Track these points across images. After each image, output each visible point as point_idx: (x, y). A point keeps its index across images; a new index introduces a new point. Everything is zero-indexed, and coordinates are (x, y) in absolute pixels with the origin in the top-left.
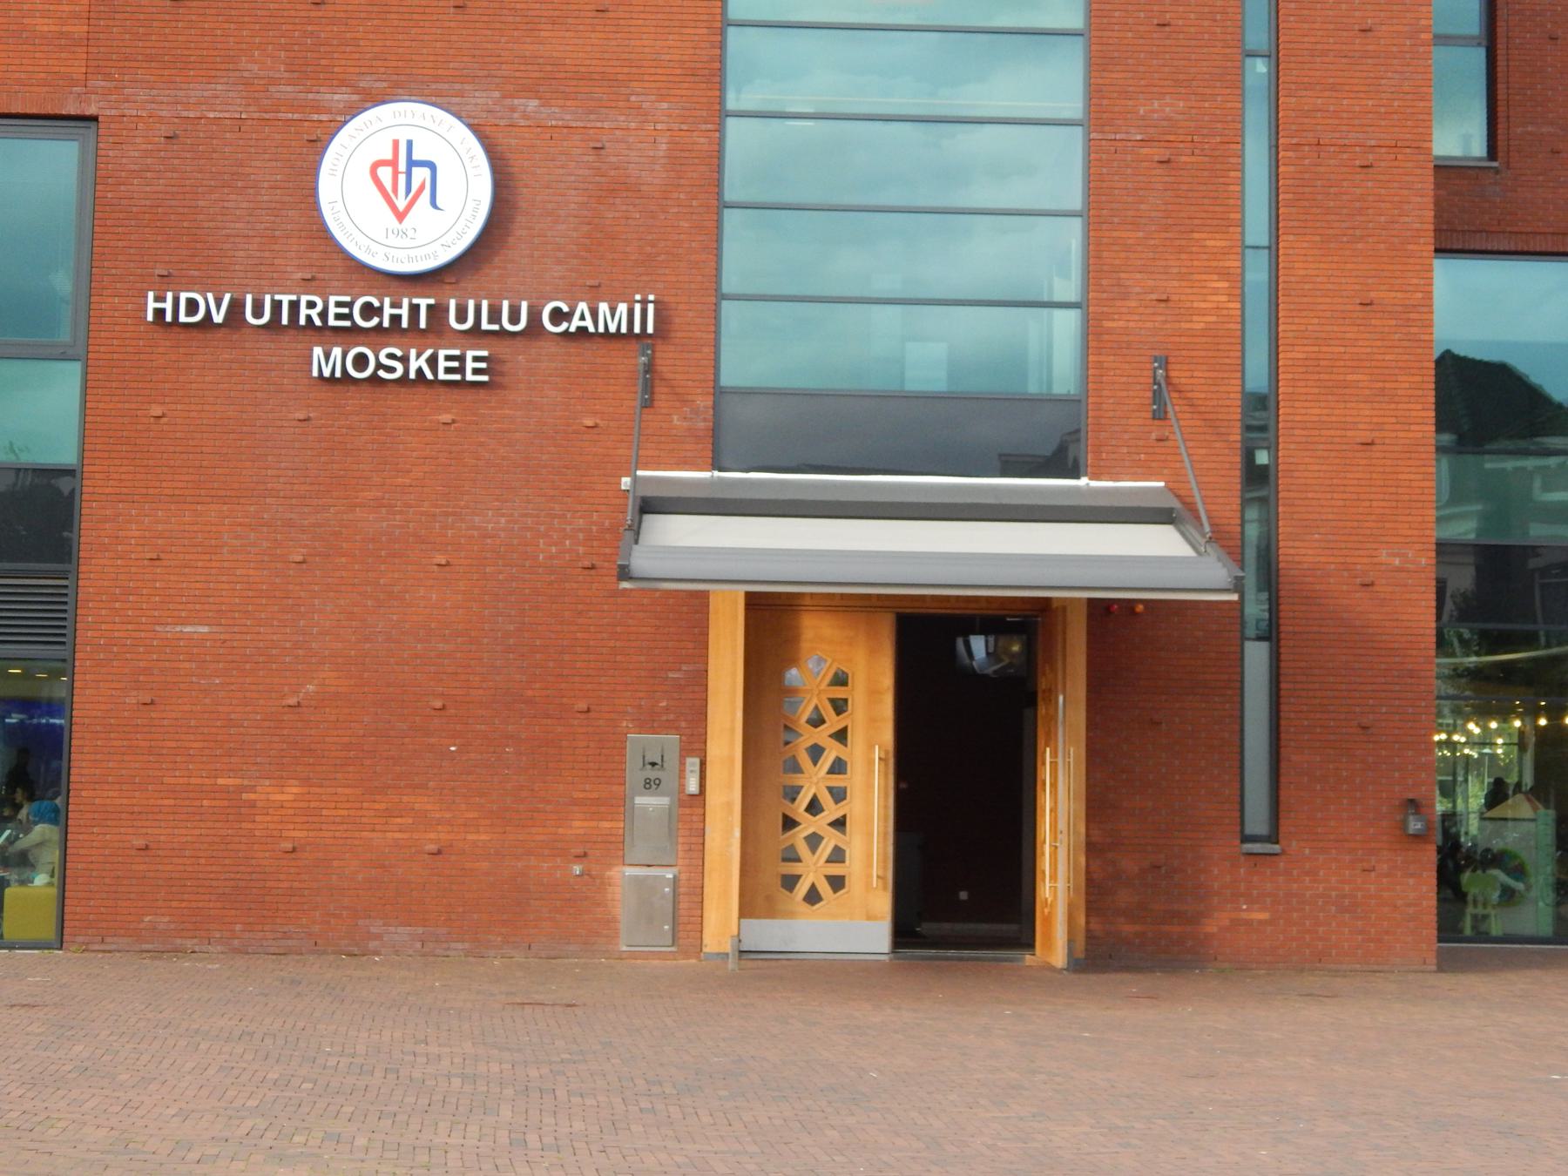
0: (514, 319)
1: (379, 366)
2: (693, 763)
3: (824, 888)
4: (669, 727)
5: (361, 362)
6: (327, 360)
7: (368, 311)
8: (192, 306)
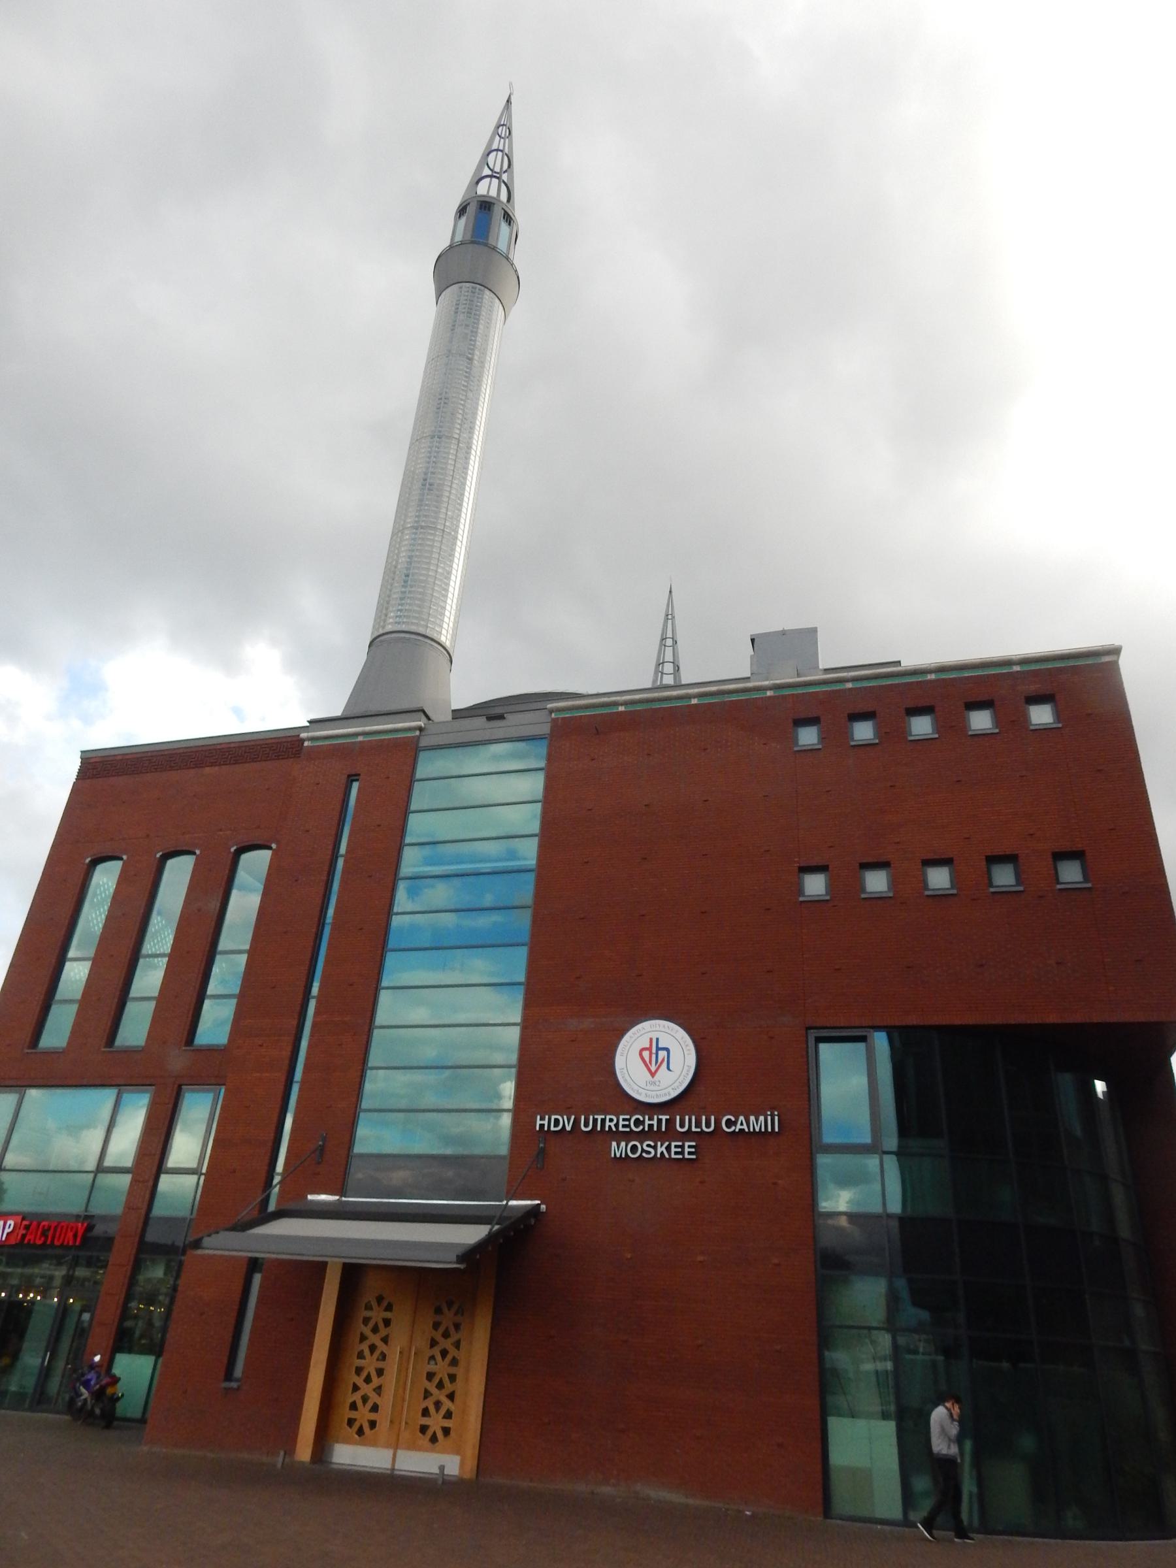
1: (643, 1150)
6: (618, 1149)
7: (638, 1123)
8: (557, 1122)
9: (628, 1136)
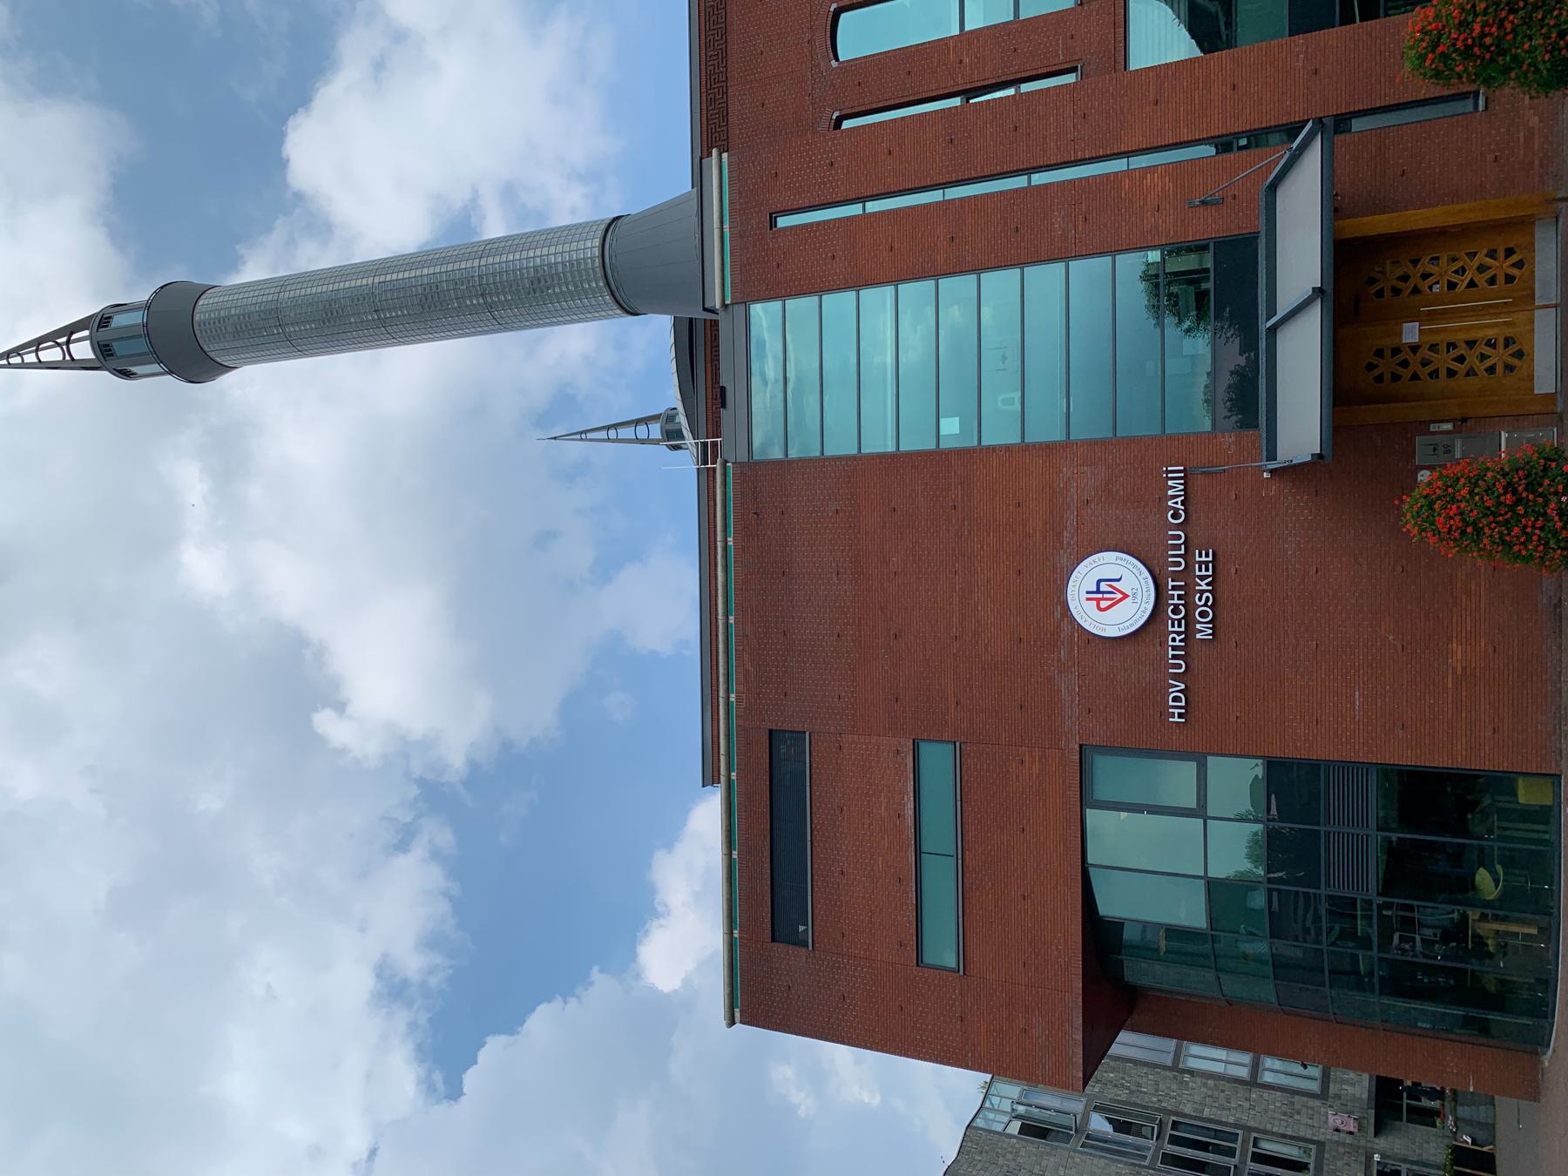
0: (1179, 537)
2: (1433, 428)
3: (1513, 349)
4: (1412, 442)
5: (1203, 614)
6: (1203, 631)
8: (1176, 699)
9: (1189, 620)
